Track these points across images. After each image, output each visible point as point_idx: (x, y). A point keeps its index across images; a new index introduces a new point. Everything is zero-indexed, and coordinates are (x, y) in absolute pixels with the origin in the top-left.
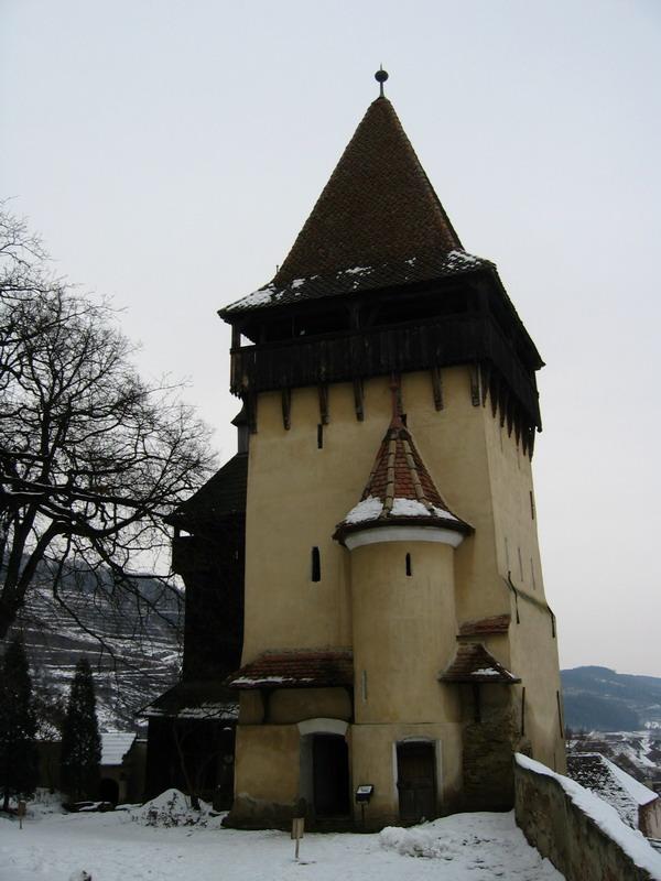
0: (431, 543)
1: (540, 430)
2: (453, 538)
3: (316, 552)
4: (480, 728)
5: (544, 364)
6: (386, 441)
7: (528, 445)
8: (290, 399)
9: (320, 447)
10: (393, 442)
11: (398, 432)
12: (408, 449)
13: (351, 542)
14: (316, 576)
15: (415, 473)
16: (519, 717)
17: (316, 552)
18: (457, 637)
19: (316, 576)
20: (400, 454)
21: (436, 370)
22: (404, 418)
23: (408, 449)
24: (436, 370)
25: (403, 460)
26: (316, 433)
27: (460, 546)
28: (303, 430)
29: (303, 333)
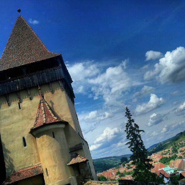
0: (58, 128)
1: (75, 98)
2: (63, 126)
3: (24, 139)
4: (81, 176)
5: (73, 81)
6: (40, 103)
7: (73, 102)
8: (9, 97)
9: (20, 109)
10: (42, 104)
11: (43, 101)
12: (47, 105)
13: (35, 133)
14: (25, 145)
15: (50, 111)
16: (89, 169)
17: (24, 139)
18: (70, 152)
19: (25, 145)
20: (44, 106)
21: (50, 83)
22: (43, 97)
23: (47, 105)
24: (50, 83)
25: (46, 107)
26: (18, 105)
27: (65, 127)
28: (14, 105)
29: (10, 78)
